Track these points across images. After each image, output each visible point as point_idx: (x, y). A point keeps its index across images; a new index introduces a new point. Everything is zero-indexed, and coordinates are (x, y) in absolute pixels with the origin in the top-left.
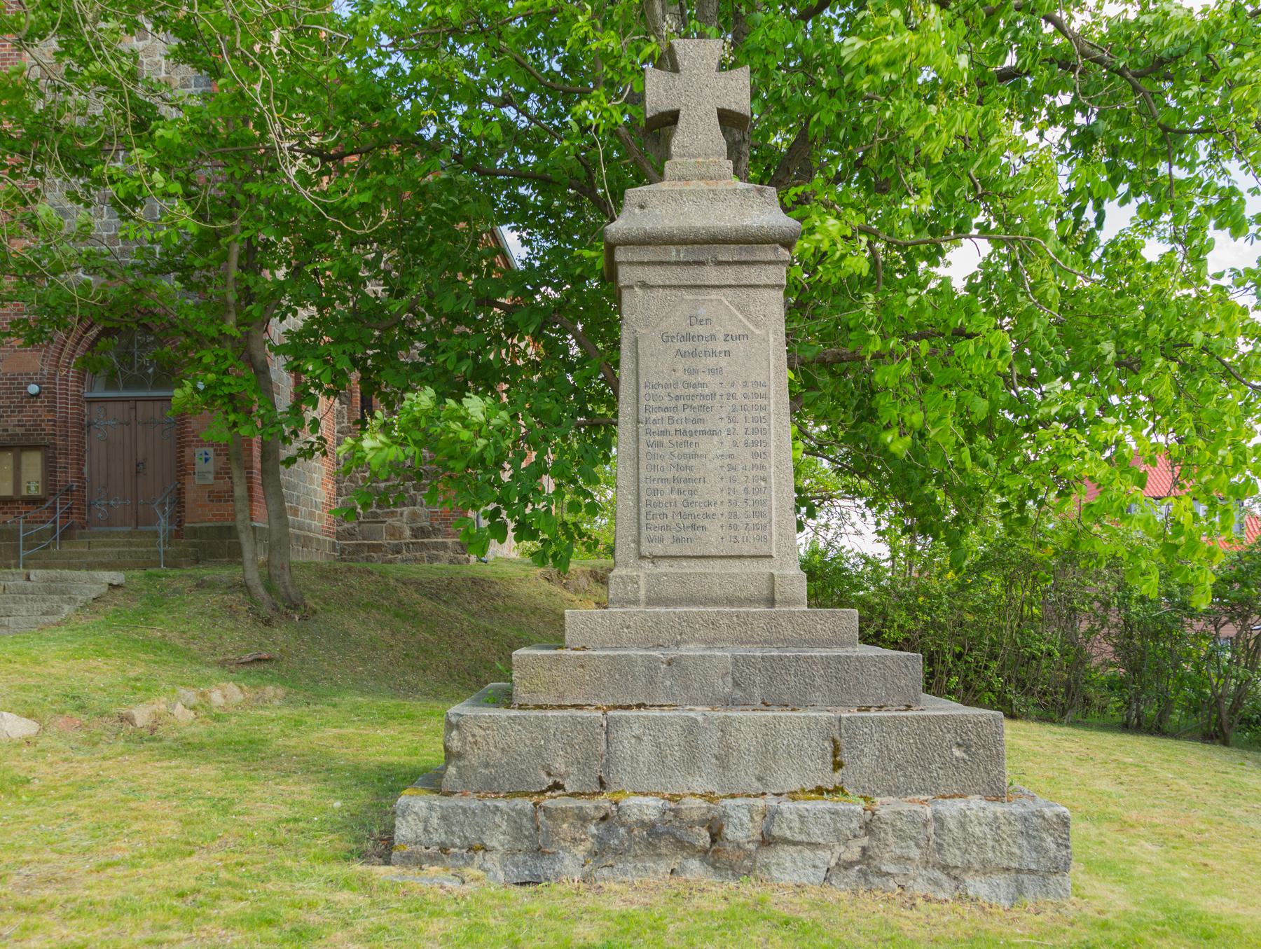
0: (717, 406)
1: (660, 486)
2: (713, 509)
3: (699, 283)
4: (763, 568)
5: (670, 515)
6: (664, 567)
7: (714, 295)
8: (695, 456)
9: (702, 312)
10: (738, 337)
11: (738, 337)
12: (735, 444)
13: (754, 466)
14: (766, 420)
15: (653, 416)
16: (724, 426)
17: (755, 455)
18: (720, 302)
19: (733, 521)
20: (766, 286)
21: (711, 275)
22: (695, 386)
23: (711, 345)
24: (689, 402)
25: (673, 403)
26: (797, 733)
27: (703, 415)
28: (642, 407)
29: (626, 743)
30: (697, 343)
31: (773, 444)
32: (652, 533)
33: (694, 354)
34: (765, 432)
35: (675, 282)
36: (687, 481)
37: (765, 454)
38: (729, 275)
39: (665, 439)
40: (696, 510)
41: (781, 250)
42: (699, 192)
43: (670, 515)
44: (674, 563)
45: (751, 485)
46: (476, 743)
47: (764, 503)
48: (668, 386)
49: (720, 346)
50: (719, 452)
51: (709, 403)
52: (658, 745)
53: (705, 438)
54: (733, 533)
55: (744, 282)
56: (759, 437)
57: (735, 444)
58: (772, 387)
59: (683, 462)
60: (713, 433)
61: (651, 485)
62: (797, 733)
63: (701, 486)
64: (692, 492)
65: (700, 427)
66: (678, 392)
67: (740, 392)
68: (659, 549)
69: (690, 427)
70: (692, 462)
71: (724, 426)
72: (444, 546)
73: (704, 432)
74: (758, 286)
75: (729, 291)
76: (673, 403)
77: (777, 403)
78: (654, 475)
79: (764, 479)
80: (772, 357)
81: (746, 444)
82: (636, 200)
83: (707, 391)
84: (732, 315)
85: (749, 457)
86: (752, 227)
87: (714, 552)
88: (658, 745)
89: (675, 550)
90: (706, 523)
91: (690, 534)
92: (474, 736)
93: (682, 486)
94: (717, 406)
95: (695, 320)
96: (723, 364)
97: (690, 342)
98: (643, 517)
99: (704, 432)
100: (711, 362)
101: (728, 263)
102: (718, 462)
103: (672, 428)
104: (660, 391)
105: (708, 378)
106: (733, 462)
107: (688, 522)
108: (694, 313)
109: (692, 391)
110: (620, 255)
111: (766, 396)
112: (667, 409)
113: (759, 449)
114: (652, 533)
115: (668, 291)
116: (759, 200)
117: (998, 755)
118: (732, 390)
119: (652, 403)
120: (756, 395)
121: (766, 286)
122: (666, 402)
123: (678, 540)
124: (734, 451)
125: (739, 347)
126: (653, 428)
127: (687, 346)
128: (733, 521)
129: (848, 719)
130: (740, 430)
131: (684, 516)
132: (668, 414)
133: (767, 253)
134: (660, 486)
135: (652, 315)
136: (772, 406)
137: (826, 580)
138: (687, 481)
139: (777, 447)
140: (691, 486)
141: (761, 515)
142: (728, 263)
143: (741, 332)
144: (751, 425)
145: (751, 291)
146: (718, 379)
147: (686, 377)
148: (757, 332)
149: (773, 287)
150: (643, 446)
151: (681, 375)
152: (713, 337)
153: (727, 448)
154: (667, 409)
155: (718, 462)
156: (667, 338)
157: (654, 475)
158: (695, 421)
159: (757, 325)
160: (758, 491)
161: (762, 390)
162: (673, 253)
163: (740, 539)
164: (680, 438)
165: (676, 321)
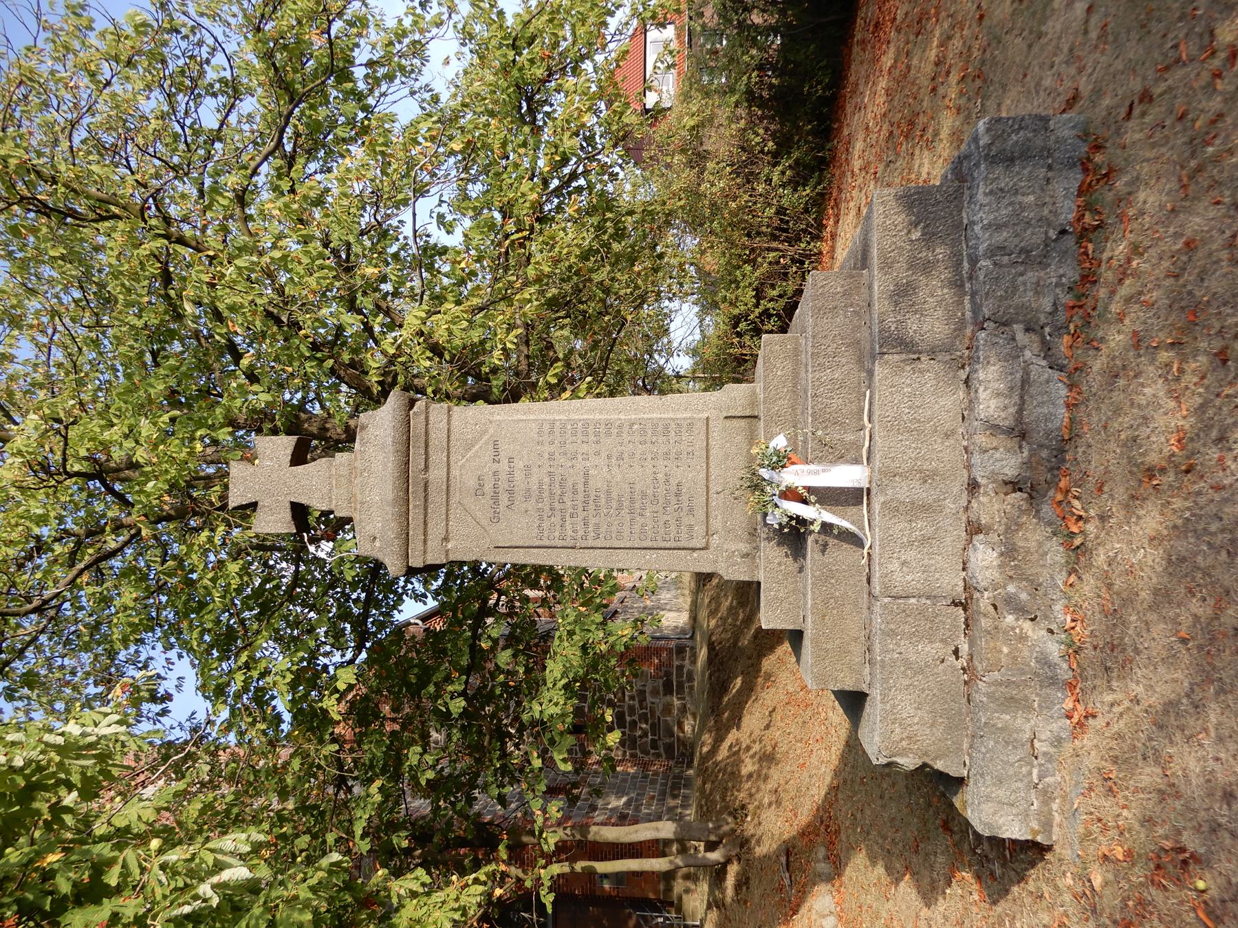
0: (560, 470)
1: (637, 527)
2: (660, 476)
3: (444, 487)
4: (717, 427)
5: (666, 518)
6: (716, 524)
7: (455, 472)
8: (608, 492)
9: (472, 483)
10: (496, 449)
11: (496, 449)
12: (597, 453)
13: (619, 434)
14: (575, 422)
15: (570, 533)
16: (580, 464)
17: (608, 434)
18: (463, 466)
19: (673, 455)
20: (449, 423)
21: (437, 474)
22: (541, 491)
23: (503, 476)
24: (557, 498)
25: (558, 513)
26: (898, 398)
27: (570, 484)
28: (561, 543)
29: (909, 578)
30: (501, 490)
31: (598, 416)
32: (684, 536)
33: (511, 492)
34: (586, 424)
35: (443, 510)
36: (632, 501)
37: (608, 424)
38: (437, 457)
39: (593, 521)
40: (661, 491)
41: (415, 409)
42: (359, 484)
43: (666, 518)
44: (712, 514)
45: (637, 438)
46: (909, 738)
47: (655, 426)
48: (541, 518)
49: (504, 466)
50: (605, 469)
51: (558, 478)
52: (911, 543)
53: (591, 482)
54: (684, 456)
55: (445, 444)
56: (591, 429)
57: (597, 453)
58: (543, 416)
59: (614, 504)
60: (586, 475)
61: (636, 536)
62: (898, 398)
63: (638, 487)
64: (644, 495)
65: (581, 487)
66: (547, 508)
67: (547, 449)
68: (699, 530)
69: (580, 496)
70: (614, 495)
71: (580, 464)
72: (680, 668)
73: (586, 483)
74: (449, 430)
75: (452, 459)
76: (558, 513)
77: (559, 413)
78: (626, 533)
79: (632, 425)
80: (516, 418)
81: (597, 442)
82: (368, 546)
83: (547, 480)
84: (476, 455)
85: (609, 441)
86: (394, 437)
87: (703, 475)
88: (911, 543)
89: (700, 514)
90: (674, 482)
91: (684, 498)
92: (902, 739)
93: (637, 505)
94: (560, 470)
95: (479, 491)
96: (521, 465)
97: (499, 496)
98: (668, 545)
99: (586, 483)
100: (519, 476)
101: (426, 460)
102: (615, 470)
103: (582, 515)
104: (545, 525)
105: (534, 479)
106: (615, 455)
107: (673, 500)
108: (472, 492)
109: (546, 494)
110: (416, 562)
111: (553, 423)
112: (563, 519)
113: (602, 429)
114: (684, 536)
115: (451, 517)
116: (371, 429)
117: (918, 193)
118: (546, 456)
119: (557, 534)
120: (551, 432)
121: (449, 423)
122: (556, 520)
123: (691, 510)
124: (604, 455)
125: (505, 448)
126: (581, 533)
127: (504, 499)
128: (673, 455)
129: (881, 347)
130: (585, 448)
131: (668, 502)
132: (568, 518)
133: (417, 423)
134: (637, 527)
135: (471, 537)
136: (562, 417)
137: (728, 365)
138: (632, 501)
139: (600, 413)
140: (637, 497)
141: (666, 427)
142: (426, 460)
143: (491, 447)
144: (580, 438)
145: (452, 437)
146: (535, 470)
147: (533, 501)
148: (491, 431)
149: (449, 416)
150: (598, 543)
151: (531, 505)
152: (495, 473)
153: (602, 461)
154: (563, 519)
155: (615, 470)
156: (496, 518)
157: (626, 533)
158: (575, 492)
159: (486, 431)
160: (643, 432)
161: (546, 427)
162: (415, 515)
163: (690, 449)
164: (592, 506)
165: (481, 508)
